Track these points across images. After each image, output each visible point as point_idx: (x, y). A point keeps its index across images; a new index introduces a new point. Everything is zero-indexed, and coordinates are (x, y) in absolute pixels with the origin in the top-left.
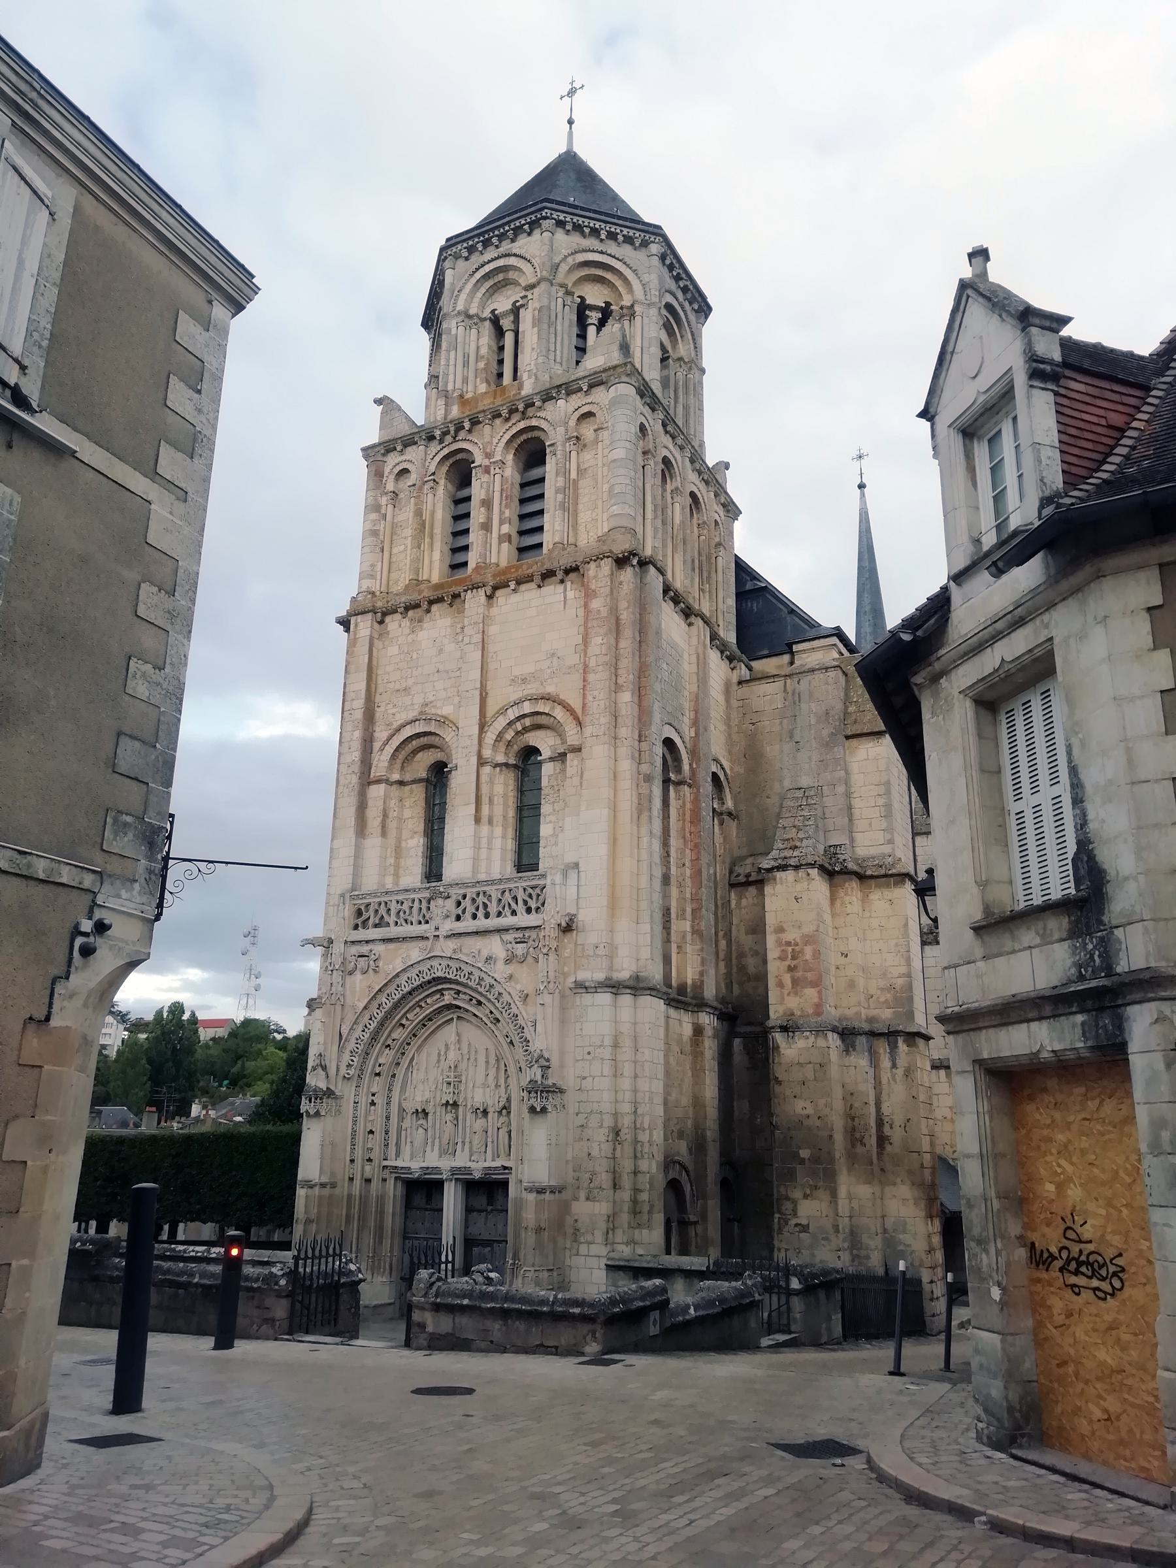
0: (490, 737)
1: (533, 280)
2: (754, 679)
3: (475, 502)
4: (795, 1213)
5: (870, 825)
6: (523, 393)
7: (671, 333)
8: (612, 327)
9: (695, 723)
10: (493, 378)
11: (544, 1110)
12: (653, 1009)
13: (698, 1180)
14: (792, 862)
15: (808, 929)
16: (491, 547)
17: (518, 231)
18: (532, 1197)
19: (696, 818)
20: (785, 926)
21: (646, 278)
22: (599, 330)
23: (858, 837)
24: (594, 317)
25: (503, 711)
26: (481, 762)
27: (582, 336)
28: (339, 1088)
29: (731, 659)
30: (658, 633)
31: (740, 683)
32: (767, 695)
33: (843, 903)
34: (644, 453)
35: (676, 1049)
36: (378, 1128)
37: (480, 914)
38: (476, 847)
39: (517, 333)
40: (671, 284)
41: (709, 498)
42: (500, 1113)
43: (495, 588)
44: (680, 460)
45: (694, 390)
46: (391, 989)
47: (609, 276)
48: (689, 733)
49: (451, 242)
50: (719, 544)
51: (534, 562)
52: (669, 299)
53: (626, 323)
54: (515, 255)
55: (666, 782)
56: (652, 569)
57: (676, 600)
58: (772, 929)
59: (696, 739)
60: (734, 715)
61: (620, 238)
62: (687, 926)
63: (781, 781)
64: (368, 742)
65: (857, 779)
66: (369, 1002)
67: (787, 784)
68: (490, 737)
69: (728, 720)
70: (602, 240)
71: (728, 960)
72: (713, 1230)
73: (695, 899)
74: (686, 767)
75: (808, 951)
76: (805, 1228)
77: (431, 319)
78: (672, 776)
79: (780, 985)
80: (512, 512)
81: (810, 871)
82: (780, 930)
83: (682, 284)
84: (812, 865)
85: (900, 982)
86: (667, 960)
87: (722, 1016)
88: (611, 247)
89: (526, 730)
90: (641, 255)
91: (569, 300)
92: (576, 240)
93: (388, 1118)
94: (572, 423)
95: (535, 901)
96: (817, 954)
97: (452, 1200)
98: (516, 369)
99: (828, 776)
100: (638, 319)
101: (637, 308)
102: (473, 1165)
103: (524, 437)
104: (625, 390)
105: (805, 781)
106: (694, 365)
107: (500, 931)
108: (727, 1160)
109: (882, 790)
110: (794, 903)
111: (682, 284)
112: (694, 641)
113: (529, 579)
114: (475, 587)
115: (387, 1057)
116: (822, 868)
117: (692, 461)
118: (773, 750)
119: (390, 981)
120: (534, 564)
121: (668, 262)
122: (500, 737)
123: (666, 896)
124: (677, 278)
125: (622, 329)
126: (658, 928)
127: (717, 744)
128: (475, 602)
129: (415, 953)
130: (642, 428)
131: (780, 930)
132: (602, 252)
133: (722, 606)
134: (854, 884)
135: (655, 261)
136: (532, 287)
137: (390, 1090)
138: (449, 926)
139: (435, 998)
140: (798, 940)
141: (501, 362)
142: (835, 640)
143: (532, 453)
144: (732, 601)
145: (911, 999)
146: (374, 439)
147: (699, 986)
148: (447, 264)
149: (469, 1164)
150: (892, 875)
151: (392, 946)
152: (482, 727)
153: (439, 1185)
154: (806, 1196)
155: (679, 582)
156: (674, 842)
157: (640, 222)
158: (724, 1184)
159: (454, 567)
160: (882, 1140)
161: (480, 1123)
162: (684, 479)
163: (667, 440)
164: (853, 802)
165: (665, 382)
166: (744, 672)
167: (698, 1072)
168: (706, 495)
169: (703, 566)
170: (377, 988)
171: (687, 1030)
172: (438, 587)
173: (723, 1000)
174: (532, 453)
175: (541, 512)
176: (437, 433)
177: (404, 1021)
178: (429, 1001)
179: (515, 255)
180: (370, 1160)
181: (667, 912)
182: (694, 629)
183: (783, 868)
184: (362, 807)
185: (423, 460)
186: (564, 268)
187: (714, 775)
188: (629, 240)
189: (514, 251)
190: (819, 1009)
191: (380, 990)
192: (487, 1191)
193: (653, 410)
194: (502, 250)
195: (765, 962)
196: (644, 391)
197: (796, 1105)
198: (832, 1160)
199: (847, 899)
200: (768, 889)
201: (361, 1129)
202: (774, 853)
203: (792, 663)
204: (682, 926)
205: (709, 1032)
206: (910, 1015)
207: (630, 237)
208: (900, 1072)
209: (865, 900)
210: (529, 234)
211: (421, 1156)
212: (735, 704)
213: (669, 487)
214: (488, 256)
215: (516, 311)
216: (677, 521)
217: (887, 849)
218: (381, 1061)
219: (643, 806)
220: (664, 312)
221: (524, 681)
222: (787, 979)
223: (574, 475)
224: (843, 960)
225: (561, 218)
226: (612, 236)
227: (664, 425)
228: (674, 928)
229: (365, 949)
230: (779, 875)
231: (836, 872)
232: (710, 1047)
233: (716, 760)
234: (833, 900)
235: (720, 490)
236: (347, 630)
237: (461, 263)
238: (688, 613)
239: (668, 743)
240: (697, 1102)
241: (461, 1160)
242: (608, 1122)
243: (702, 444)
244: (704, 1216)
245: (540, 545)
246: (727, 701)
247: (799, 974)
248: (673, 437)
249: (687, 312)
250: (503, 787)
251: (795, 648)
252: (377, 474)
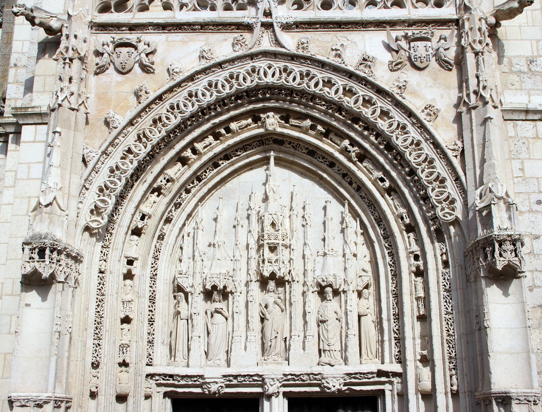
36: (139, 311)
42: (360, 294)
46: (180, 96)
66: (139, 115)
93: (152, 300)
102: (326, 371)
115: (155, 206)
119: (179, 85)
129: (222, 46)
137: (156, 258)
139: (244, 122)
149: (317, 369)
170: (152, 96)
177: (188, 153)
178: (234, 126)
180: (124, 364)
191: (160, 98)
201: (113, 312)
218: (145, 208)
229: (132, 37)
241: (303, 362)
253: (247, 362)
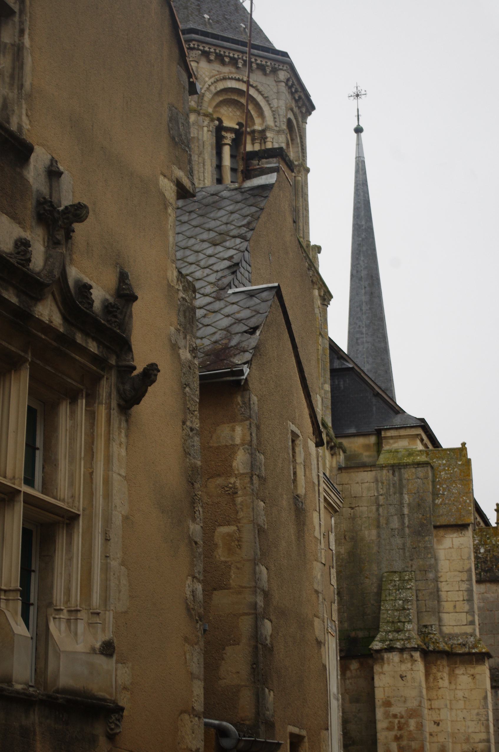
5: (455, 607)
14: (398, 645)
15: (412, 704)
20: (392, 701)
21: (275, 103)
23: (445, 617)
24: (229, 137)
33: (435, 679)
58: (381, 702)
65: (444, 565)
70: (238, 68)
75: (412, 723)
81: (413, 653)
82: (388, 704)
84: (415, 649)
85: (481, 746)
90: (270, 81)
92: (217, 67)
96: (420, 726)
101: (269, 134)
109: (465, 576)
131: (388, 704)
135: (283, 87)
140: (403, 713)
142: (420, 431)
150: (474, 654)
164: (440, 585)
183: (390, 649)
199: (439, 674)
200: (377, 668)
207: (263, 65)
209: (452, 674)
224: (435, 728)
225: (207, 49)
230: (386, 655)
234: (427, 674)
247: (404, 743)
251: (383, 434)
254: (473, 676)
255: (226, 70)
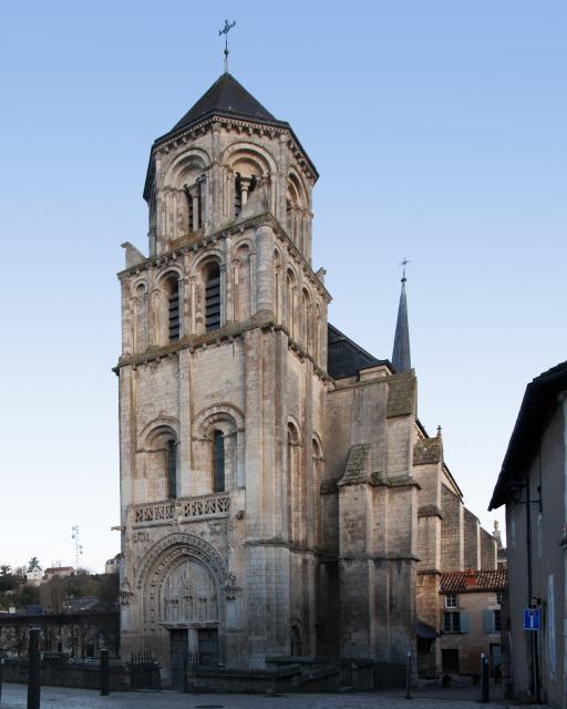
0: (196, 426)
1: (208, 164)
2: (337, 389)
3: (181, 301)
4: (350, 638)
6: (206, 235)
7: (293, 193)
8: (259, 192)
9: (305, 414)
10: (187, 227)
11: (234, 598)
12: (286, 551)
13: (306, 624)
14: (354, 481)
16: (193, 326)
17: (198, 132)
18: (229, 634)
19: (305, 462)
21: (278, 158)
22: (249, 195)
24: (246, 185)
25: (202, 412)
26: (193, 439)
27: (239, 198)
28: (136, 591)
29: (324, 380)
30: (285, 367)
31: (329, 392)
32: (345, 397)
34: (278, 267)
35: (294, 569)
37: (197, 513)
38: (195, 481)
39: (199, 198)
40: (294, 162)
41: (315, 288)
43: (195, 348)
44: (297, 269)
45: (306, 227)
47: (254, 158)
48: (301, 419)
49: (158, 142)
50: (319, 317)
51: (217, 332)
52: (292, 170)
53: (266, 188)
54: (197, 149)
55: (290, 444)
56: (282, 333)
57: (294, 349)
59: (304, 423)
60: (324, 408)
61: (262, 132)
62: (300, 514)
63: (350, 442)
64: (134, 433)
67: (353, 443)
68: (196, 426)
69: (321, 412)
70: (250, 135)
71: (319, 530)
72: (313, 646)
73: (304, 501)
74: (300, 437)
76: (355, 644)
77: (150, 193)
78: (292, 442)
79: (345, 540)
80: (203, 304)
82: (346, 514)
83: (300, 160)
84: (364, 483)
86: (290, 531)
87: (316, 555)
88: (255, 139)
89: (215, 421)
91: (230, 175)
92: (233, 134)
94: (235, 252)
95: (225, 505)
96: (365, 525)
97: (192, 637)
98: (200, 221)
99: (376, 438)
100: (273, 186)
101: (272, 178)
103: (210, 260)
104: (267, 229)
105: (362, 442)
106: (306, 211)
107: (207, 520)
108: (318, 617)
110: (352, 500)
111: (300, 160)
112: (305, 371)
113: (213, 342)
114: (184, 348)
116: (370, 483)
117: (304, 270)
118: (345, 426)
120: (217, 334)
121: (292, 146)
122: (201, 426)
123: (289, 500)
124: (297, 157)
125: (264, 192)
126: (286, 515)
127: (317, 425)
128: (185, 356)
129: (165, 531)
130: (276, 252)
131: (346, 514)
132: (250, 143)
133: (321, 350)
134: (387, 490)
135: (284, 146)
136: (208, 169)
138: (180, 519)
141: (191, 217)
143: (213, 270)
144: (325, 349)
145: (410, 543)
146: (123, 267)
147: (305, 541)
148: (156, 157)
151: (155, 529)
152: (192, 421)
153: (186, 631)
154: (355, 631)
155: (296, 340)
156: (293, 475)
157: (274, 120)
158: (317, 627)
159: (172, 337)
160: (391, 606)
161: (204, 605)
162: (300, 280)
163: (291, 259)
165: (289, 225)
166: (332, 387)
167: (305, 580)
168: (312, 289)
169: (310, 330)
171: (300, 561)
172: (165, 348)
173: (316, 548)
174: (213, 270)
175: (218, 304)
176: (158, 262)
179: (197, 149)
181: (289, 508)
182: (305, 364)
183: (349, 484)
184: (133, 464)
185: (153, 278)
186: (226, 155)
187: (314, 440)
188: (267, 133)
189: (197, 146)
190: (364, 549)
192: (208, 633)
193: (282, 241)
194: (188, 145)
195: (338, 529)
196: (277, 230)
197: (350, 593)
198: (368, 615)
202: (344, 478)
203: (358, 380)
204: (297, 515)
205: (310, 562)
206: (409, 550)
208: (402, 576)
210: (204, 134)
211: (177, 620)
212: (325, 403)
213: (291, 286)
214: (180, 150)
215: (199, 185)
216: (296, 304)
217: (404, 473)
219: (279, 456)
220: (289, 180)
221: (213, 396)
222: (349, 537)
223: (237, 282)
226: (256, 131)
227: (289, 250)
228: (293, 515)
231: (377, 484)
232: (311, 569)
233: (315, 433)
235: (320, 286)
236: (118, 374)
237: (165, 157)
238: (301, 356)
239: (291, 425)
240: (305, 593)
242: (264, 602)
243: (310, 260)
244: (308, 640)
245: (219, 323)
246: (322, 403)
247: (355, 534)
248: (294, 256)
249: (303, 178)
250: (204, 452)
252: (126, 288)
253: (182, 621)
254: (404, 498)
255: (243, 136)
